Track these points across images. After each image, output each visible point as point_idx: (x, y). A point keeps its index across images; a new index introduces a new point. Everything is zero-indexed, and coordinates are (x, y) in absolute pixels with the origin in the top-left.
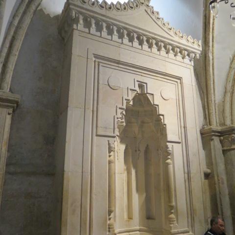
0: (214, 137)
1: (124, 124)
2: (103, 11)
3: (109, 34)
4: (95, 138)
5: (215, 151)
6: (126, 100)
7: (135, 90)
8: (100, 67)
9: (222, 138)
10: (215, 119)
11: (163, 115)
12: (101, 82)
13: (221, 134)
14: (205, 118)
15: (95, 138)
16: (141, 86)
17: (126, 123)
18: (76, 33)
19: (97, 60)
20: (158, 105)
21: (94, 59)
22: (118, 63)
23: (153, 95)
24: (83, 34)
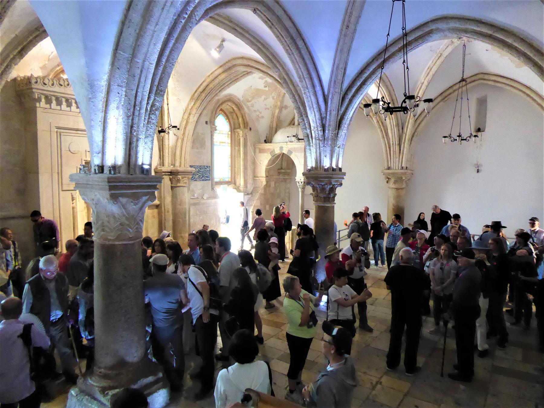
0: (164, 177)
2: (62, 90)
3: (68, 106)
4: (61, 192)
5: (164, 188)
8: (62, 136)
9: (171, 177)
10: (167, 161)
12: (63, 149)
13: (171, 173)
14: (160, 158)
15: (61, 192)
18: (39, 111)
19: (59, 130)
21: (56, 130)
22: (76, 130)
24: (46, 110)
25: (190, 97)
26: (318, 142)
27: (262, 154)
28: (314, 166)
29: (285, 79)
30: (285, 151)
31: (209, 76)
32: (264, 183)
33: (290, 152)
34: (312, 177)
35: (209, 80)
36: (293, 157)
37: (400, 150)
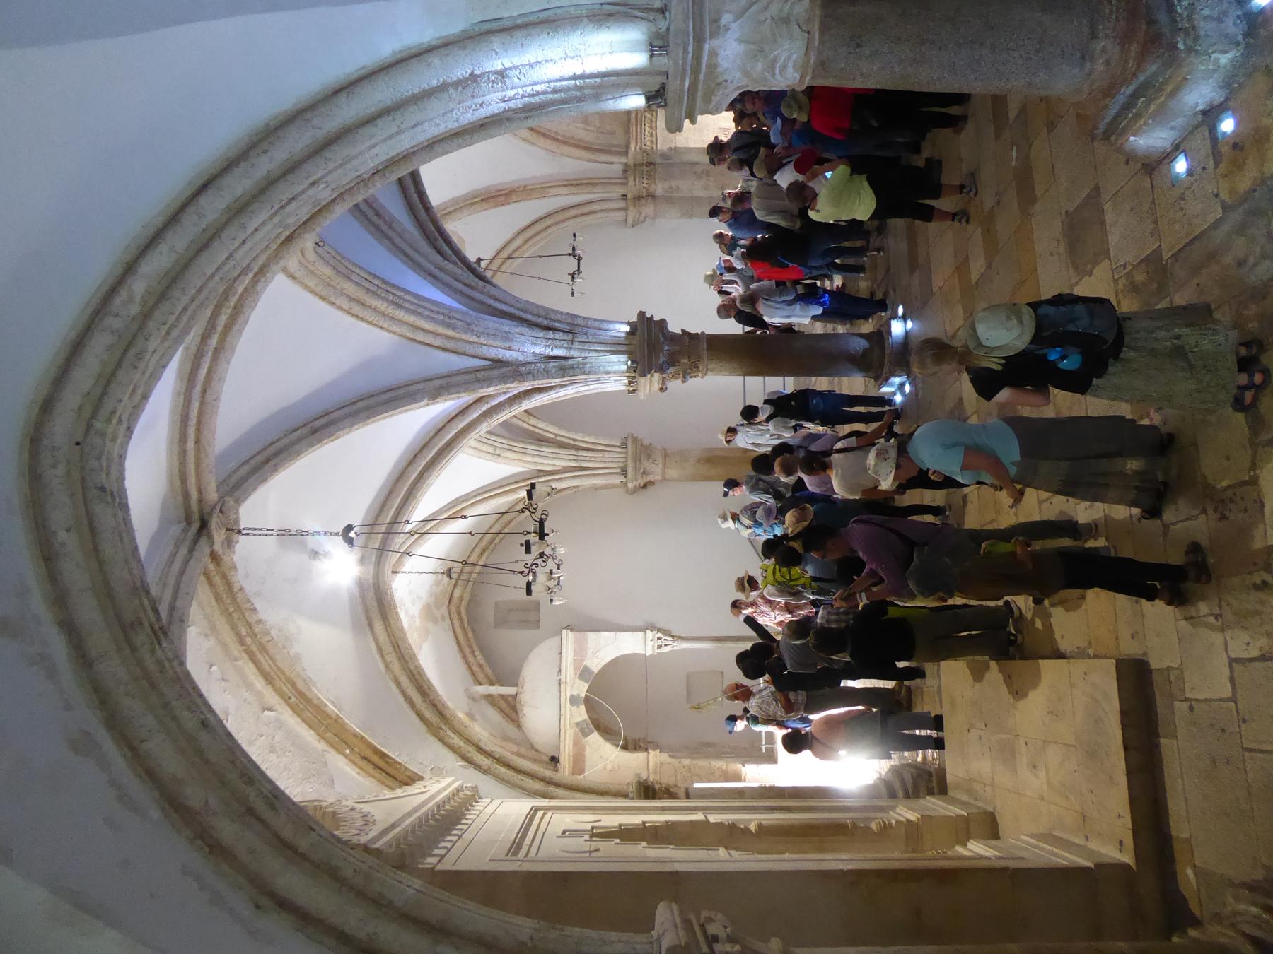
25: (432, 739)
26: (576, 345)
27: (588, 763)
28: (623, 358)
29: (441, 387)
30: (582, 689)
31: (387, 666)
32: (664, 757)
33: (584, 673)
34: (650, 357)
35: (396, 667)
36: (596, 664)
37: (588, 449)
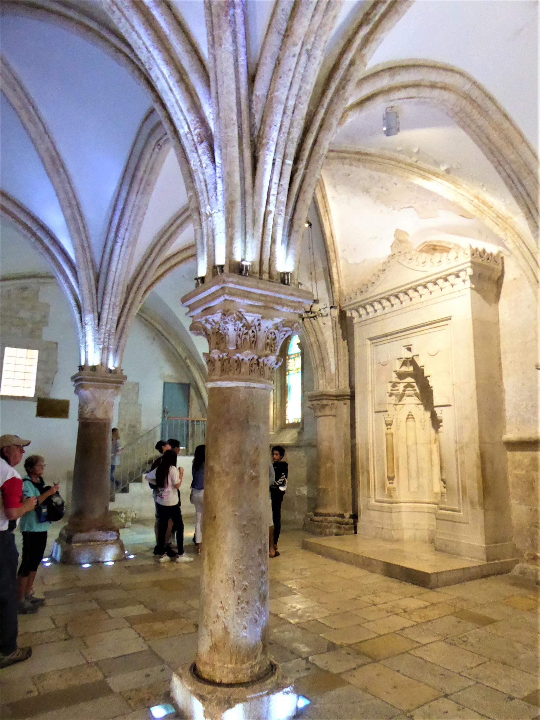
1: (418, 391)
6: (394, 371)
7: (402, 358)
11: (429, 376)
16: (409, 349)
17: (420, 390)
20: (423, 366)
21: (369, 342)
23: (418, 355)
